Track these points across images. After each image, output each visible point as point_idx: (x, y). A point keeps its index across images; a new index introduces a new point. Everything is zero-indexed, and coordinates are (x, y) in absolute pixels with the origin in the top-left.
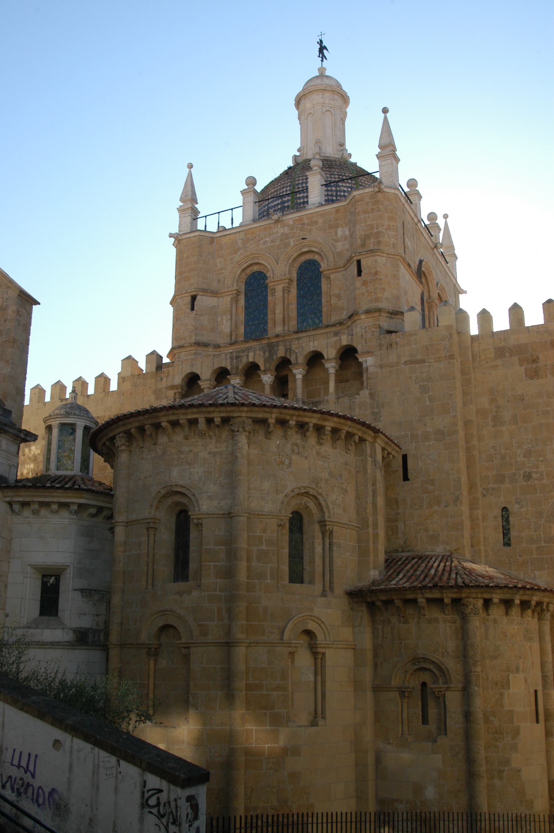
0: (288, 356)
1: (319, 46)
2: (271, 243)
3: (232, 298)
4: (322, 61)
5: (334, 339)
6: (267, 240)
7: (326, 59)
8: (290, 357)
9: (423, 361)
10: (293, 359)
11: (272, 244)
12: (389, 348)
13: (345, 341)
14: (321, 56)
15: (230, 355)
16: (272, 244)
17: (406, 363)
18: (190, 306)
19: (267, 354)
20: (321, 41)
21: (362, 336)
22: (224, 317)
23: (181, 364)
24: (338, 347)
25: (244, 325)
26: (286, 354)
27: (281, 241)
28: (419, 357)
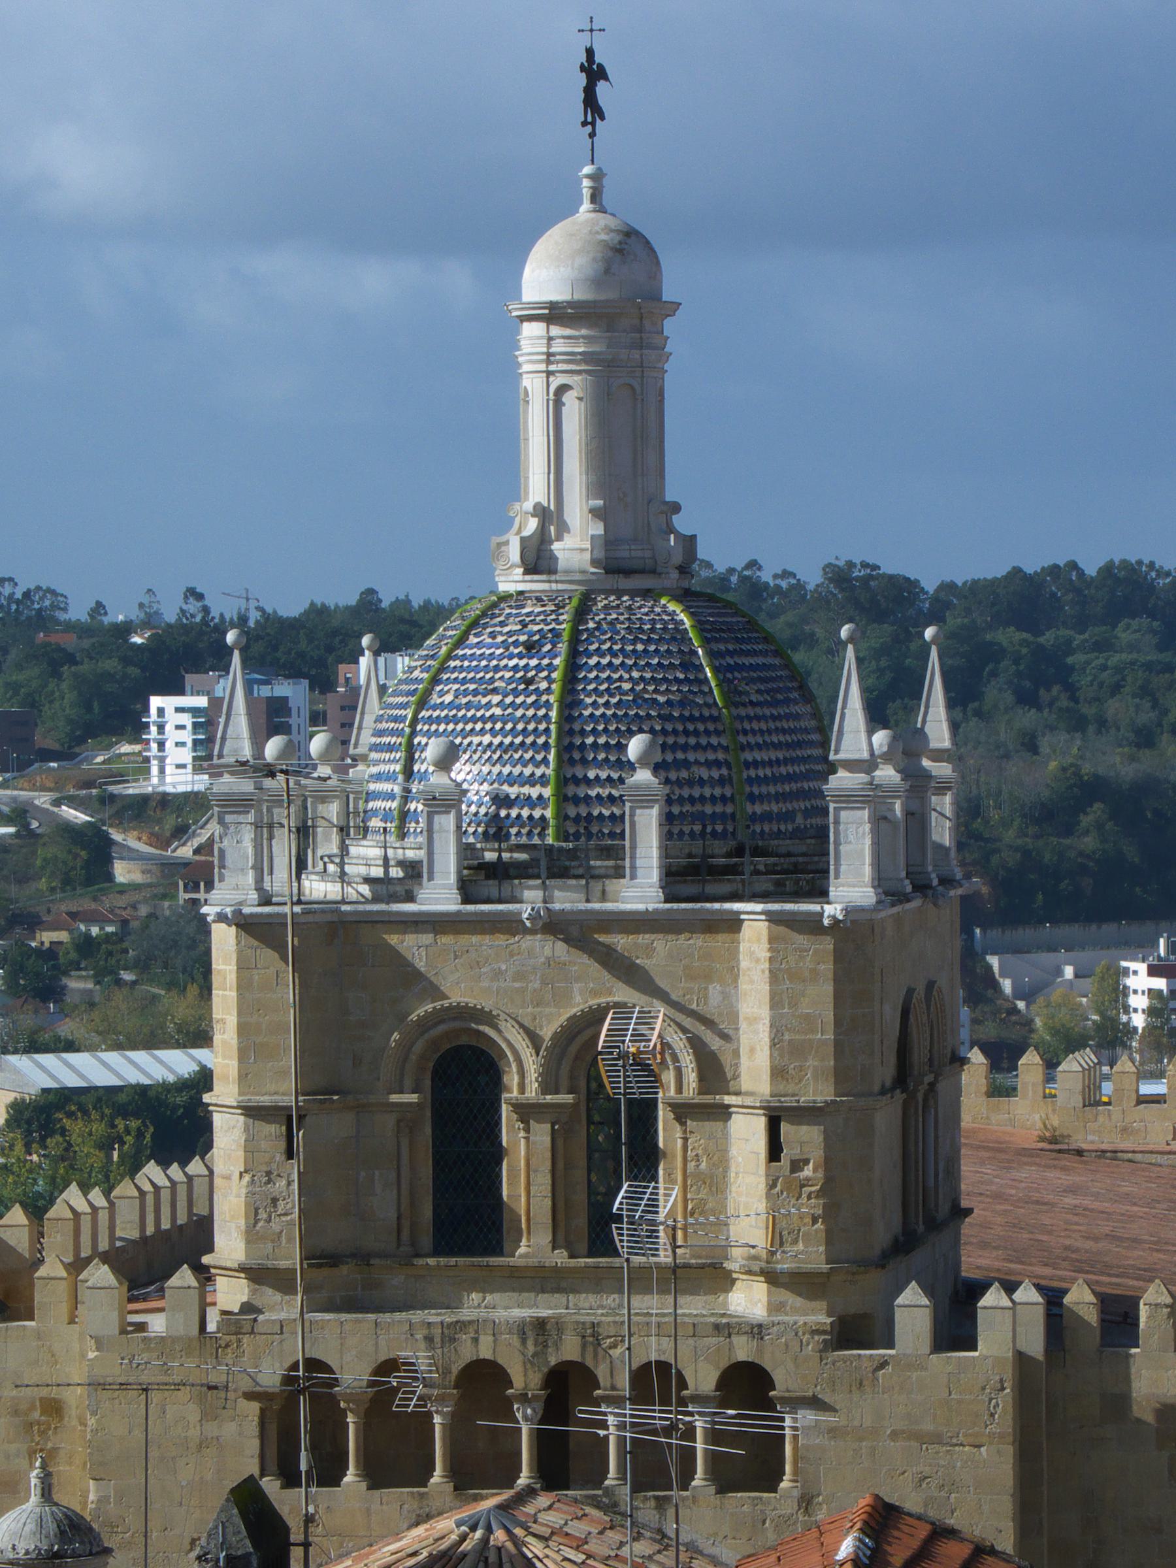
0: (589, 1363)
1: (582, 79)
2: (514, 981)
3: (399, 1121)
4: (592, 135)
5: (714, 1340)
6: (504, 967)
7: (602, 118)
8: (596, 1367)
9: (936, 1439)
10: (602, 1372)
11: (517, 985)
12: (854, 1388)
13: (743, 1349)
14: (589, 119)
15: (426, 1332)
16: (517, 985)
17: (894, 1435)
18: (282, 1145)
19: (531, 1348)
20: (590, 53)
21: (787, 1345)
22: (377, 1173)
23: (277, 1329)
24: (724, 1364)
25: (431, 1198)
26: (583, 1355)
27: (544, 983)
28: (928, 1426)
